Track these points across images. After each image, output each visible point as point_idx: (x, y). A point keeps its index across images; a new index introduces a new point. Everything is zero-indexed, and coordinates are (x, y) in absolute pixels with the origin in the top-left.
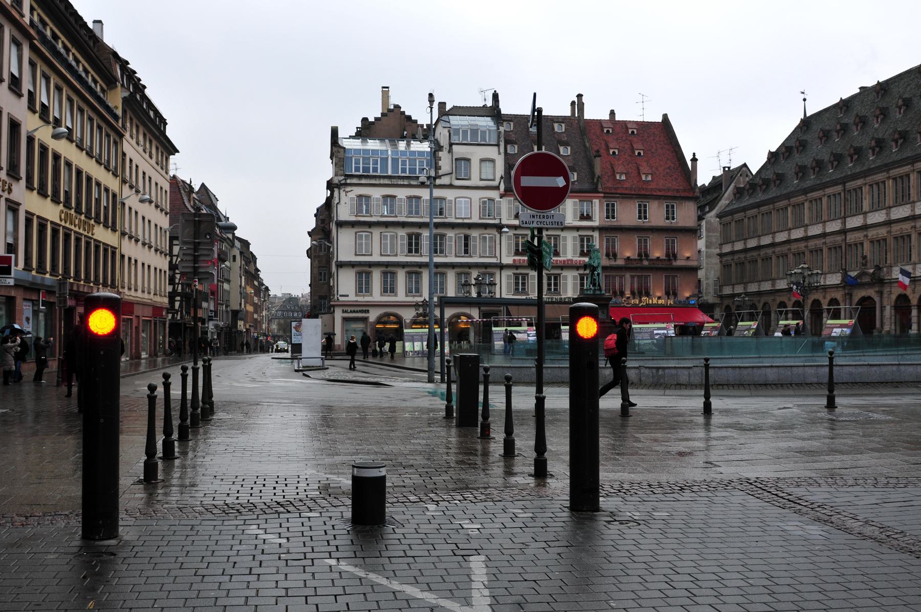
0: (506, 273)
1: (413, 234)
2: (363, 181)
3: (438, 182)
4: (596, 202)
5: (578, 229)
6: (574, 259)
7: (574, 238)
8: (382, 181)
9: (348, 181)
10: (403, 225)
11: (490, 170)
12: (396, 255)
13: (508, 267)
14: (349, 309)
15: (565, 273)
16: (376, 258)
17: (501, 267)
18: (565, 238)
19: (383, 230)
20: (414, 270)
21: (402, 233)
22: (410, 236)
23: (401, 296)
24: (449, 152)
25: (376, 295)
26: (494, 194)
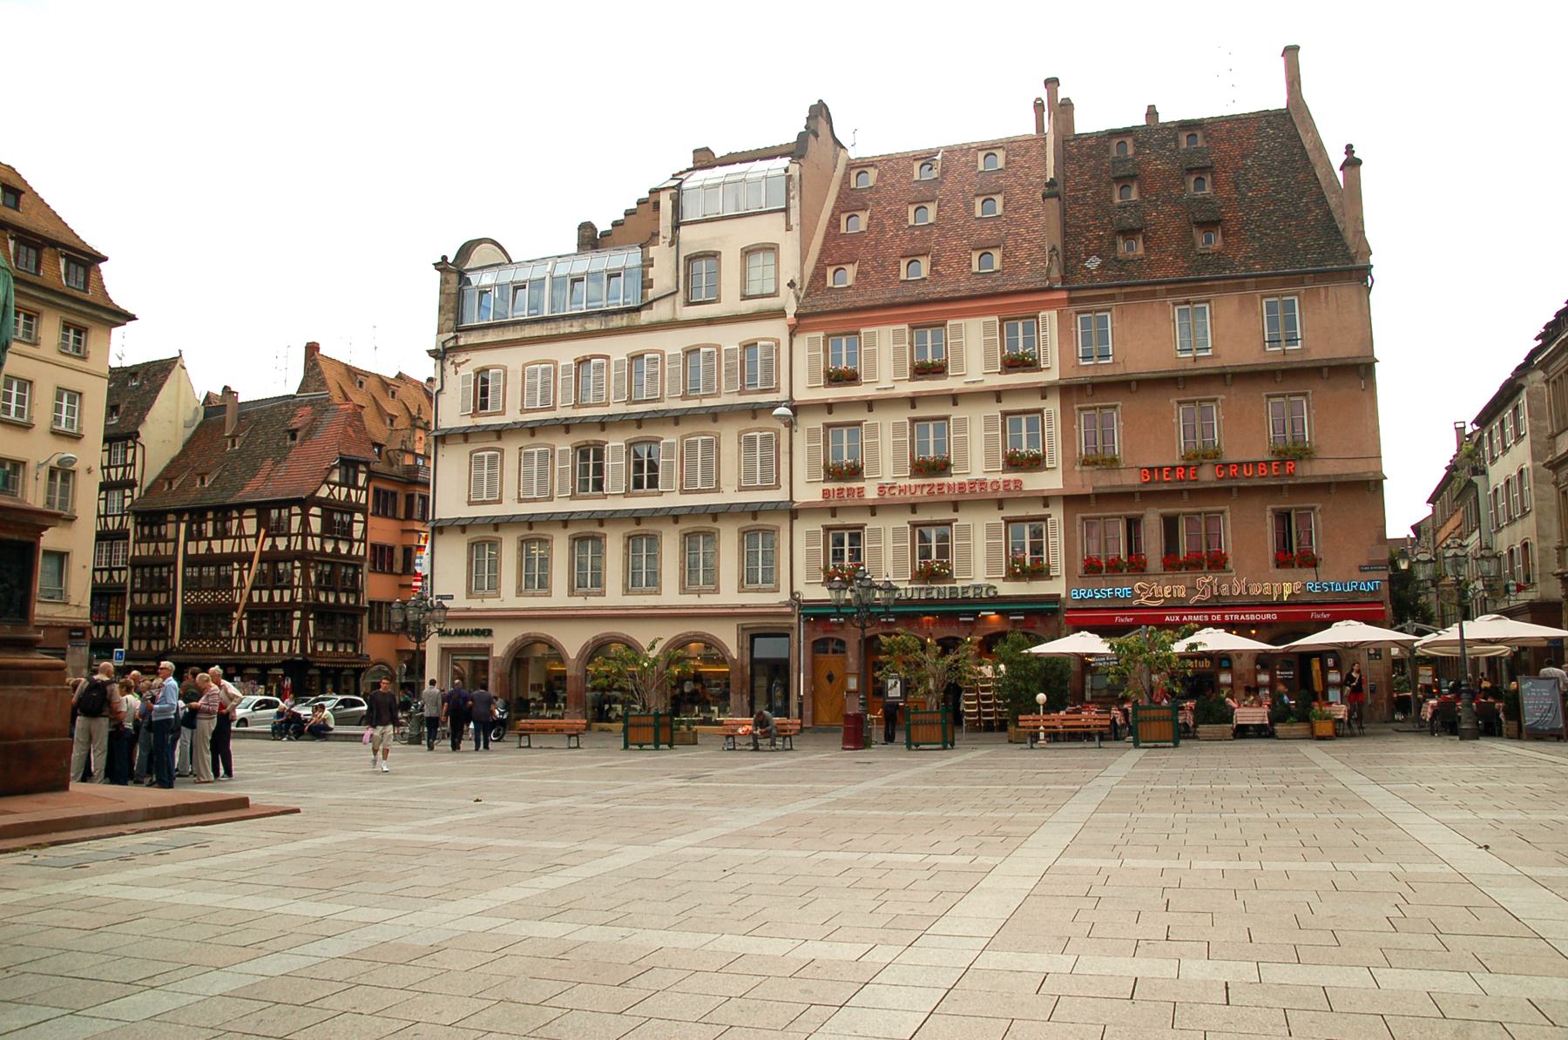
0: (803, 527)
1: (588, 445)
2: (491, 337)
3: (645, 317)
4: (1050, 318)
5: (998, 395)
6: (990, 478)
7: (988, 421)
8: (530, 332)
9: (462, 342)
10: (567, 426)
11: (771, 272)
12: (551, 499)
13: (811, 510)
14: (453, 627)
15: (963, 518)
16: (510, 508)
17: (793, 512)
18: (962, 423)
19: (525, 441)
20: (587, 533)
21: (564, 444)
22: (582, 451)
23: (559, 596)
24: (671, 244)
25: (509, 598)
26: (776, 330)
